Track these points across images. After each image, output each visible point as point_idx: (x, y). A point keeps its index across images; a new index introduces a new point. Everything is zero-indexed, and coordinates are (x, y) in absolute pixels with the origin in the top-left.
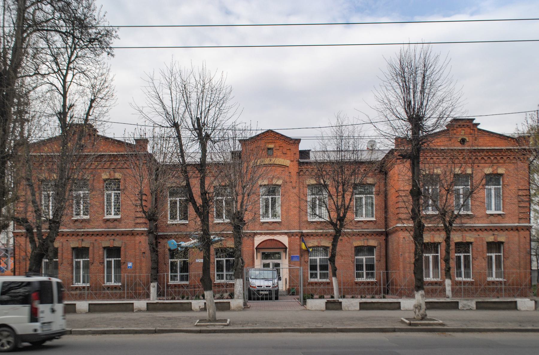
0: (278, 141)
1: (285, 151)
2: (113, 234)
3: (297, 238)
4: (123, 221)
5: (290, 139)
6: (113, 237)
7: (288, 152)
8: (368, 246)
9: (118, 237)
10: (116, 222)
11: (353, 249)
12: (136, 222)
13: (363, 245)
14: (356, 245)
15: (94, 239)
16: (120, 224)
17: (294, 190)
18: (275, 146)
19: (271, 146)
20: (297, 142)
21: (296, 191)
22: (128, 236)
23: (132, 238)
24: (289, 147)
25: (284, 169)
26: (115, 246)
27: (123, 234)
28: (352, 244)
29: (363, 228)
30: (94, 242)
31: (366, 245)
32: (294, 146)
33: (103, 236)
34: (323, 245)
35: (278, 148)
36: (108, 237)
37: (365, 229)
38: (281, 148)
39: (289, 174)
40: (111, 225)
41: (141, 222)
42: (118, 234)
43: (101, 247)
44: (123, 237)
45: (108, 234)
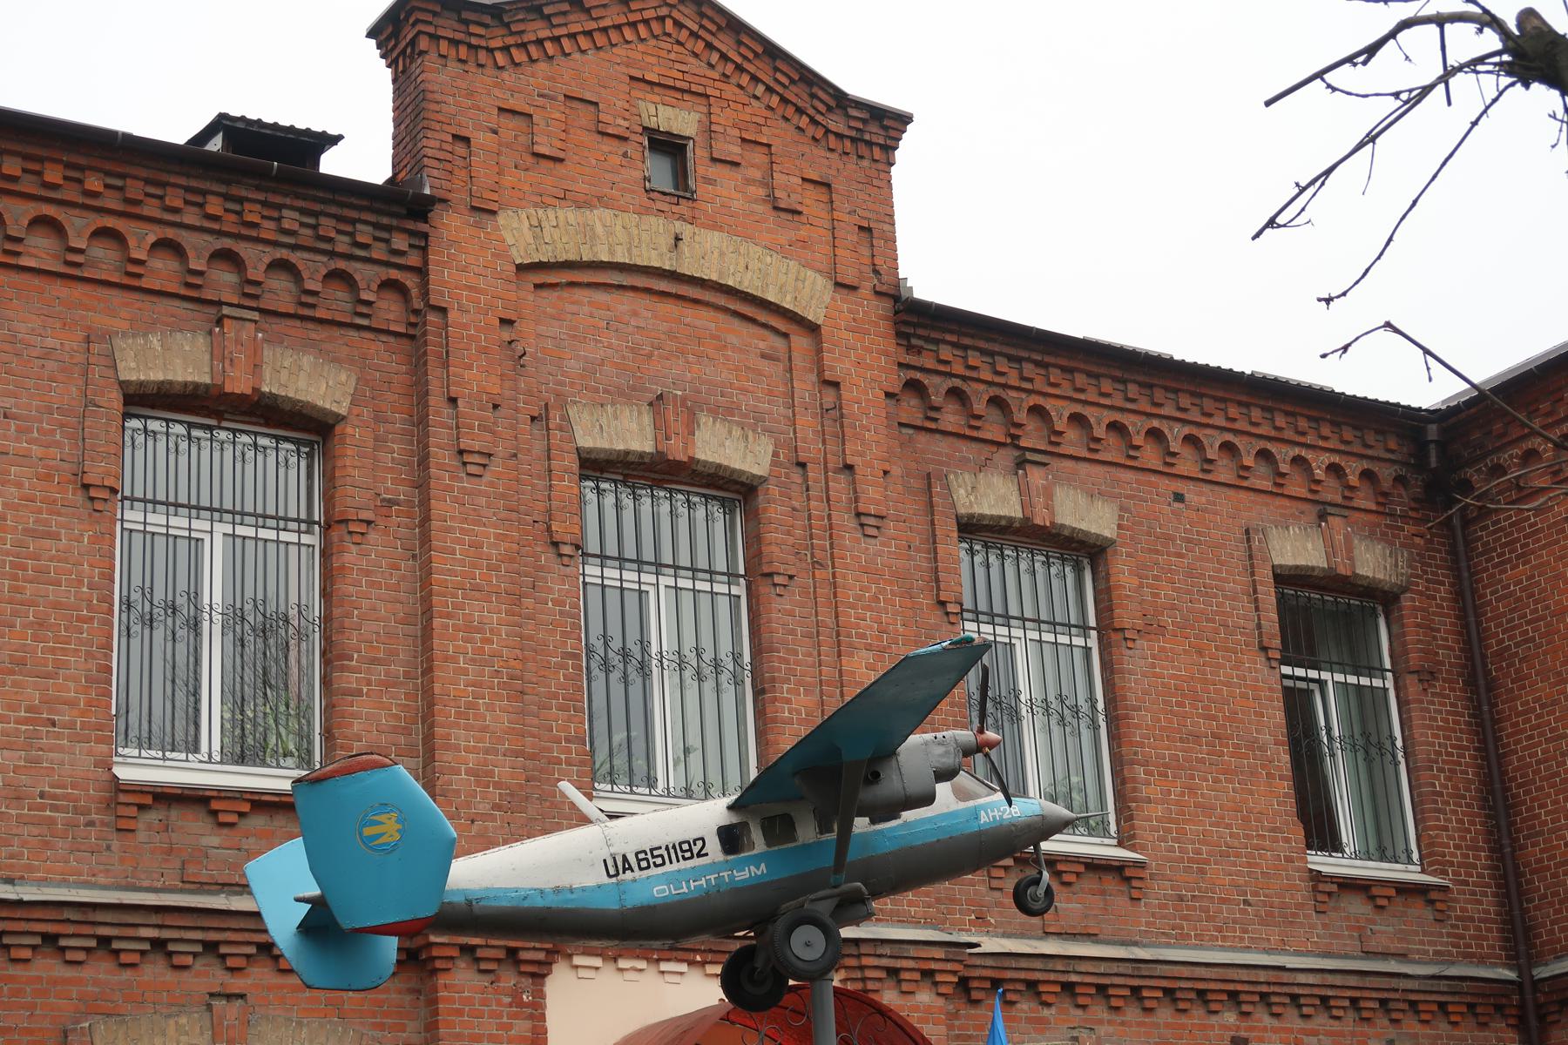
0: (730, 91)
1: (788, 185)
3: (928, 1009)
5: (841, 99)
7: (811, 201)
17: (873, 546)
18: (709, 131)
19: (680, 120)
20: (874, 133)
21: (880, 551)
24: (821, 163)
25: (779, 343)
29: (1373, 945)
32: (851, 164)
35: (734, 150)
37: (1385, 955)
38: (758, 156)
39: (829, 397)
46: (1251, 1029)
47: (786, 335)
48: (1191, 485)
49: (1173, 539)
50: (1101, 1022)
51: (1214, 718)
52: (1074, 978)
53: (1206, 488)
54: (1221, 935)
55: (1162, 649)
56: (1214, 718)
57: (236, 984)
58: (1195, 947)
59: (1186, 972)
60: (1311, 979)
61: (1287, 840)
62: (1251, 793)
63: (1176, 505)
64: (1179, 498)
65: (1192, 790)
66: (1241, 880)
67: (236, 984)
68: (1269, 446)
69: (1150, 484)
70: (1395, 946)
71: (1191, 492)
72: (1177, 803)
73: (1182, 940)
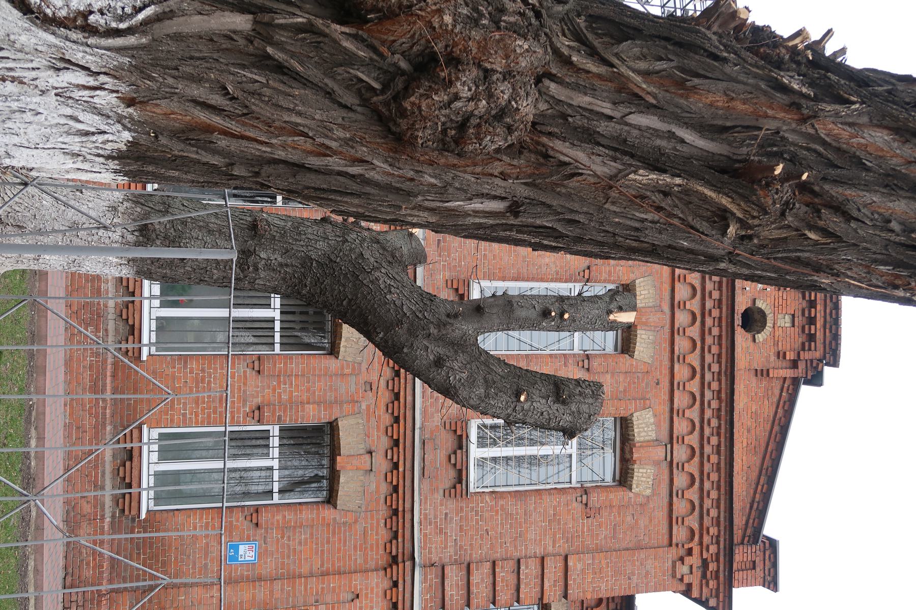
2: (396, 466)
4: (451, 504)
6: (382, 464)
9: (384, 488)
10: (452, 474)
12: (448, 570)
15: (374, 377)
16: (439, 496)
22: (384, 534)
23: (378, 557)
26: (342, 480)
27: (395, 512)
30: (364, 377)
33: (387, 419)
36: (385, 442)
40: (438, 456)
41: (448, 592)
42: (396, 489)
43: (335, 413)
44: (383, 512)
45: (396, 443)
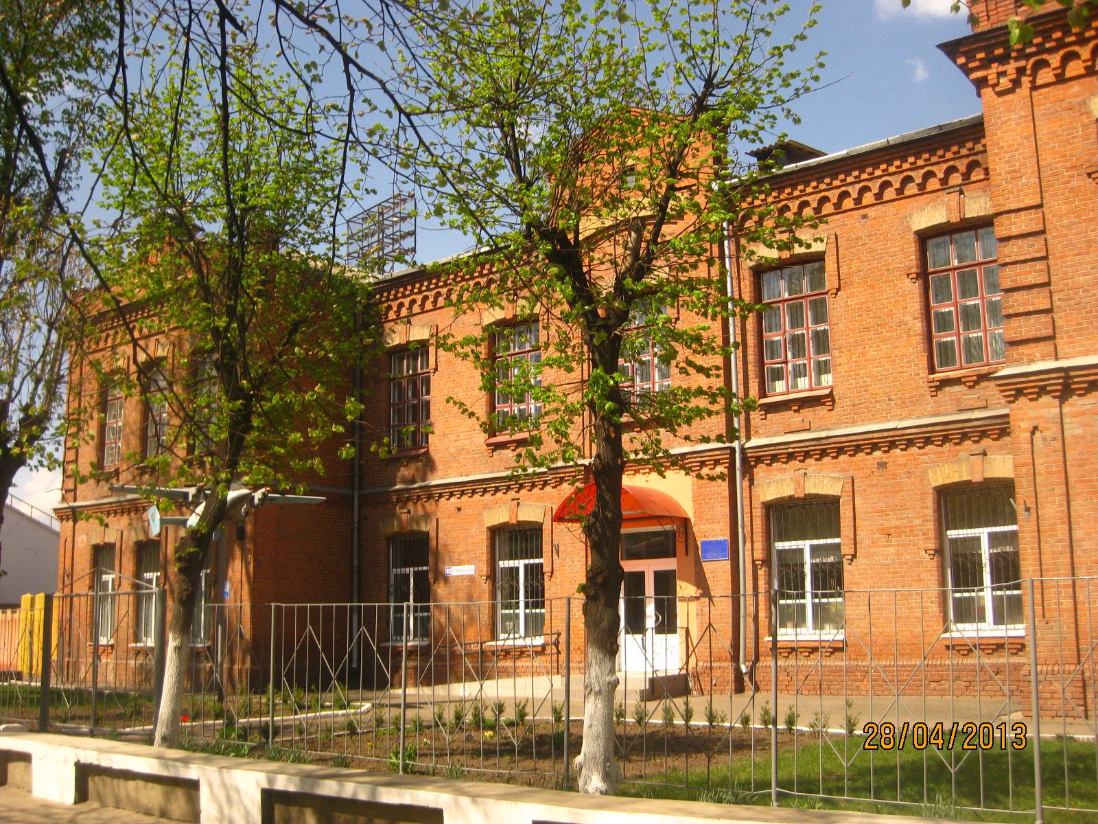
8: (988, 481)
11: (930, 501)
13: (965, 478)
14: (940, 482)
28: (923, 478)
29: (964, 406)
31: (977, 478)
34: (813, 491)
46: (889, 457)
47: (676, 223)
48: (873, 209)
49: (860, 238)
50: (811, 465)
51: (878, 317)
52: (791, 450)
53: (880, 206)
54: (875, 418)
55: (853, 292)
56: (878, 317)
57: (518, 496)
58: (851, 426)
59: (844, 439)
60: (914, 431)
61: (916, 365)
62: (897, 347)
63: (862, 221)
64: (864, 217)
65: (863, 354)
66: (888, 390)
67: (518, 496)
68: (909, 173)
69: (849, 216)
70: (983, 403)
71: (871, 212)
72: (855, 362)
73: (854, 423)
